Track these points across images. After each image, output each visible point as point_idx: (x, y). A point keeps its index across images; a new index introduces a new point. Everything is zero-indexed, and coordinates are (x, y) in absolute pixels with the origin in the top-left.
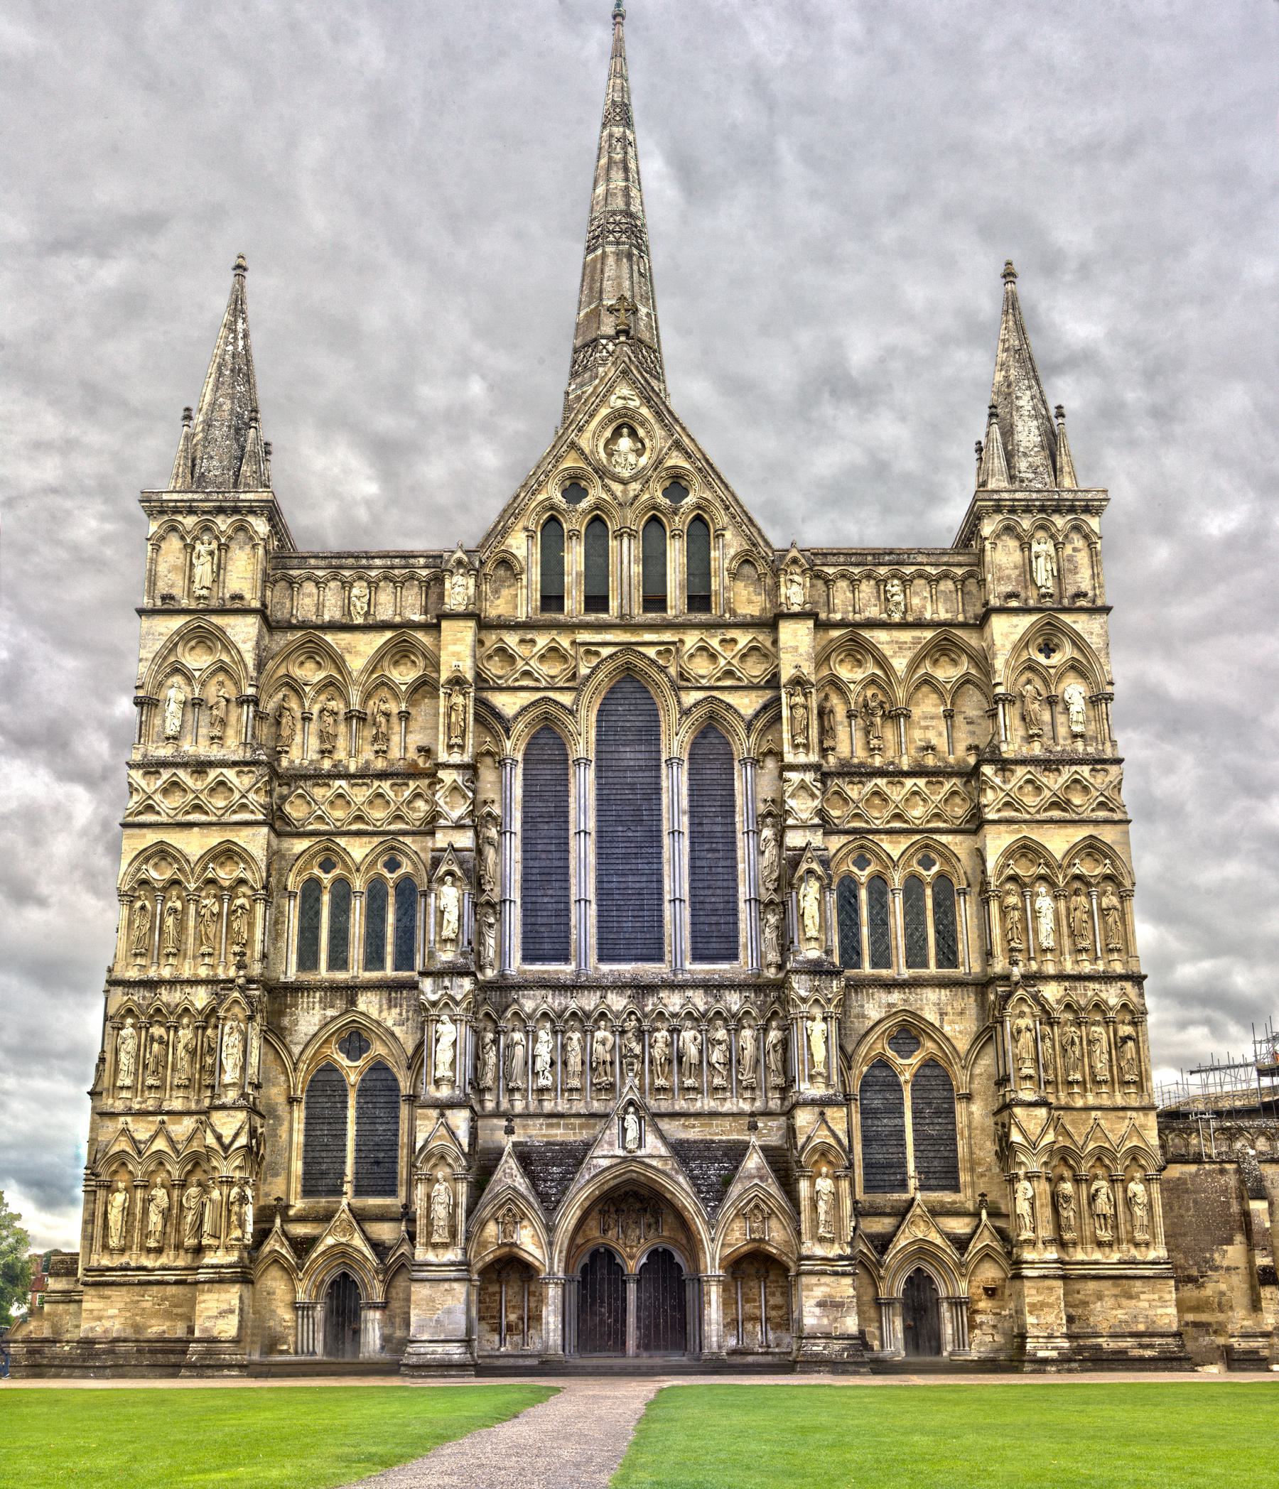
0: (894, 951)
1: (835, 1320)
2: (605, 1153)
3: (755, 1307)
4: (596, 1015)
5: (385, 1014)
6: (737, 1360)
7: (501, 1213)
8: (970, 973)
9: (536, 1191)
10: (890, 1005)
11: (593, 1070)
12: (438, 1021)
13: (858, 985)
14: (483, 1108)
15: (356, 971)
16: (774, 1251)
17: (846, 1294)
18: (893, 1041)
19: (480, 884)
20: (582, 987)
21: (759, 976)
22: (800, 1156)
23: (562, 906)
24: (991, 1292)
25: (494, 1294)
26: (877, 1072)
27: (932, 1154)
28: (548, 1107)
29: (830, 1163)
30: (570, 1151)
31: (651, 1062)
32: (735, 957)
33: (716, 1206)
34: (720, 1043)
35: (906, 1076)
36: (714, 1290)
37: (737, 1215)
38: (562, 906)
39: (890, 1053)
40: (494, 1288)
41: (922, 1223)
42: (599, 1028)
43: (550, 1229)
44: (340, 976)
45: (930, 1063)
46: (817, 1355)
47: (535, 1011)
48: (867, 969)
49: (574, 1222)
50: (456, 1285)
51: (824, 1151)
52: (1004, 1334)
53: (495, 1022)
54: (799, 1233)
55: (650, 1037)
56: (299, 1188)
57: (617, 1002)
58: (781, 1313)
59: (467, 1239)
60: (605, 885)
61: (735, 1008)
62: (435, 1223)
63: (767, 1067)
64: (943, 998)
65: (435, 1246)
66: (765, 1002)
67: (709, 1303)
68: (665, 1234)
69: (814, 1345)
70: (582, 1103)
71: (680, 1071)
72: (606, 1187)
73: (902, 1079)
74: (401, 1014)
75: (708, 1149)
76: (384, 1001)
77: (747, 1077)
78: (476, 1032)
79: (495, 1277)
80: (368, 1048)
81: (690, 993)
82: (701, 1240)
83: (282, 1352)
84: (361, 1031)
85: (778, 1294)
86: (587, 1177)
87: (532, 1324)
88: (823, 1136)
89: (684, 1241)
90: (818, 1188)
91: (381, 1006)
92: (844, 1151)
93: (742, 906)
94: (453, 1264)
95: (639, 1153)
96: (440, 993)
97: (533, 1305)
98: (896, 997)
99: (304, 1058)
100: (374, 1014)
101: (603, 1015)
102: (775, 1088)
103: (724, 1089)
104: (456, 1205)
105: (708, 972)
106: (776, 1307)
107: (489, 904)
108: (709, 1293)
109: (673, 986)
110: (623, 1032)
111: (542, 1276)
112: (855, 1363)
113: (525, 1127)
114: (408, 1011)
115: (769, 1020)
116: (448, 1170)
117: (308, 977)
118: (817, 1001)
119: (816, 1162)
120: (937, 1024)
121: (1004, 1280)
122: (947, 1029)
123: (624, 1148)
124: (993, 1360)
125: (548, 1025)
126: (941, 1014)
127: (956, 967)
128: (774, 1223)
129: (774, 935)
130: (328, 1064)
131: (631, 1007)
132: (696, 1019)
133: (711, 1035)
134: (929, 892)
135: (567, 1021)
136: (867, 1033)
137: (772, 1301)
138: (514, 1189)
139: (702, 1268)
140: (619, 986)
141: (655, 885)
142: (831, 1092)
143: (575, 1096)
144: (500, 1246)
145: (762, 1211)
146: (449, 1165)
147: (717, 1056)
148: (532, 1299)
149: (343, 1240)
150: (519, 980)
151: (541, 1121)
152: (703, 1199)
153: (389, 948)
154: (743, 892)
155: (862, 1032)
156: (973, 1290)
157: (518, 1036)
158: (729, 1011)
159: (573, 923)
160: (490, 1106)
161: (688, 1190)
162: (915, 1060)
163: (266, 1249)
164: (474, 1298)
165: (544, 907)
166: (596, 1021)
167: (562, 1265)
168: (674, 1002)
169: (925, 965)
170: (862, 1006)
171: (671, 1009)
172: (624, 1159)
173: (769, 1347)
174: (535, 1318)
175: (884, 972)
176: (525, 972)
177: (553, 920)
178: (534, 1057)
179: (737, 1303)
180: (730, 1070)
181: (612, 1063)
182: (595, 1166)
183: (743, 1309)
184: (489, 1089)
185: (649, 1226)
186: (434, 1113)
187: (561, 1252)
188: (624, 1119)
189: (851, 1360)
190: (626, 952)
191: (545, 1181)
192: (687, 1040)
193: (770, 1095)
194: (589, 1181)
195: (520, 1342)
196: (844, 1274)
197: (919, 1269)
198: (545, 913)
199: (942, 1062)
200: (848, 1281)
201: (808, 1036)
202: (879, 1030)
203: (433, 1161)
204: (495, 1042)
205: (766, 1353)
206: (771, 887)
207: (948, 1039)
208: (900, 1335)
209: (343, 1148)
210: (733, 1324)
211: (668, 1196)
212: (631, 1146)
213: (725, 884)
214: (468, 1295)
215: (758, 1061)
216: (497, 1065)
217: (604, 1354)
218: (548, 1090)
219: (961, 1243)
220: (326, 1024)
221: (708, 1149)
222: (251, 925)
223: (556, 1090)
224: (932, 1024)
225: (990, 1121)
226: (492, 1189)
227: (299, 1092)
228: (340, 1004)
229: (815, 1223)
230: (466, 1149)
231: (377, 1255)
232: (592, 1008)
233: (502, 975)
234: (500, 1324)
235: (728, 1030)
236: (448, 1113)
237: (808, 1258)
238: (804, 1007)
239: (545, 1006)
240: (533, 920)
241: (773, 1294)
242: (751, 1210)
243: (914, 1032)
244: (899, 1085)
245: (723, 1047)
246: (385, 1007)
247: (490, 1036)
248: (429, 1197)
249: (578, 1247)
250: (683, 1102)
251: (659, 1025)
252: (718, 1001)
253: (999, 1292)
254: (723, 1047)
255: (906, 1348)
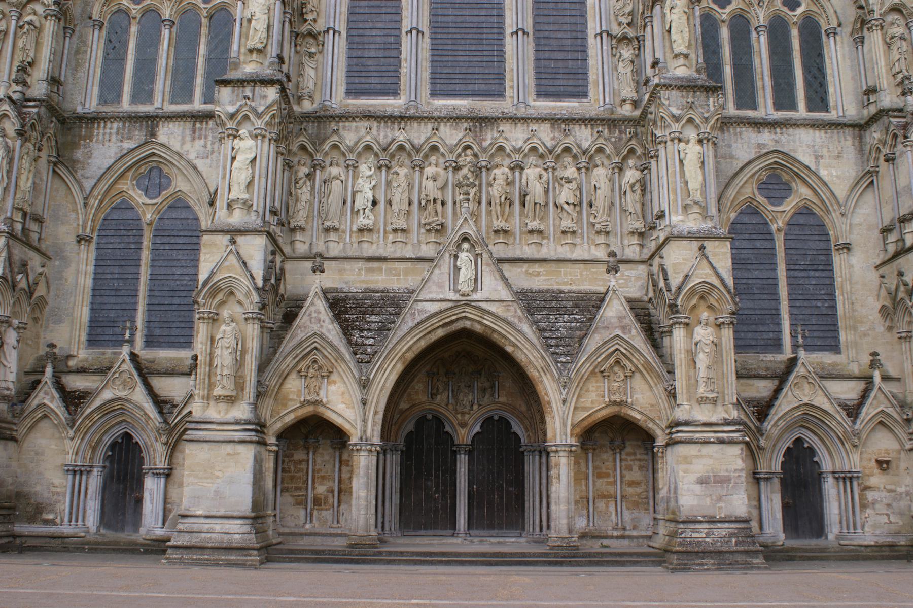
0: (760, 93)
1: (720, 499)
2: (433, 296)
3: (608, 483)
4: (426, 148)
5: (187, 146)
6: (595, 546)
7: (303, 365)
8: (844, 116)
9: (349, 341)
10: (759, 145)
11: (422, 208)
12: (235, 137)
13: (726, 123)
14: (293, 250)
15: (160, 102)
16: (638, 416)
17: (733, 467)
18: (764, 187)
19: (302, 14)
20: (411, 118)
21: (612, 113)
22: (676, 299)
23: (392, 39)
24: (883, 465)
25: (301, 462)
26: (746, 219)
27: (808, 311)
28: (369, 250)
29: (711, 307)
30: (393, 298)
31: (490, 203)
32: (585, 95)
33: (567, 362)
34: (569, 181)
35: (778, 224)
36: (563, 461)
37: (593, 373)
38: (392, 39)
39: (760, 199)
40: (299, 455)
41: (806, 386)
42: (430, 164)
43: (364, 385)
44: (143, 108)
45: (805, 211)
46: (699, 543)
47: (356, 144)
48: (732, 110)
49: (394, 377)
50: (241, 448)
51: (703, 294)
52: (901, 514)
53: (311, 156)
54: (672, 395)
55: (488, 175)
56: (84, 337)
57: (451, 135)
58: (639, 490)
59: (259, 395)
60: (440, 19)
61: (585, 145)
62: (219, 371)
63: (624, 210)
64: (818, 140)
65: (218, 399)
66: (620, 139)
67: (559, 477)
68: (503, 399)
69: (694, 531)
70: (409, 247)
71: (522, 214)
72: (434, 337)
73: (774, 227)
74: (205, 146)
75: (556, 299)
76: (188, 133)
77: (601, 219)
78: (288, 166)
79: (302, 443)
80: (169, 184)
81: (534, 126)
82: (549, 403)
83: (46, 522)
84: (163, 167)
85: (635, 468)
86: (411, 324)
87: (343, 497)
88: (703, 274)
89: (524, 408)
90: (697, 338)
91: (183, 138)
92: (729, 292)
93: (593, 45)
94: (237, 423)
95: (475, 297)
96: (239, 103)
97: (345, 476)
98: (766, 138)
99: (96, 193)
100: (176, 145)
101: (434, 149)
102: (632, 233)
103: (574, 233)
104: (244, 352)
105: (554, 108)
106: (632, 484)
107: (312, 35)
108: (558, 465)
109: (514, 120)
110: (457, 169)
111: (354, 440)
112: (746, 552)
113: (340, 271)
114: (213, 143)
115: (625, 158)
116: (238, 309)
117: (109, 109)
118: (690, 121)
119: (694, 307)
120: (813, 168)
121: (899, 452)
122: (823, 173)
123: (457, 291)
124: (892, 546)
125: (372, 158)
126: (816, 158)
127: (827, 111)
128: (638, 381)
129: (629, 70)
130: (124, 201)
131: (469, 140)
132: (542, 156)
133: (560, 173)
134: (795, 32)
135: (392, 156)
136: (736, 175)
137: (628, 477)
138: (321, 336)
139: (549, 435)
140: (455, 119)
141: (495, 19)
142: (709, 224)
143: (400, 237)
144: (302, 405)
145: (624, 368)
146: (239, 302)
147: (565, 195)
148: (344, 468)
149: (123, 394)
150: (339, 111)
151: (360, 264)
152: (553, 354)
153: (199, 80)
154: (593, 27)
155: (730, 174)
156: (865, 463)
157: (335, 171)
158: (579, 147)
159: (403, 56)
160: (301, 248)
161: (535, 340)
162: (789, 206)
163: (34, 402)
164: (269, 464)
165: (371, 39)
166: (426, 156)
167: (378, 428)
168: (516, 136)
169: (793, 107)
170: (730, 146)
171: (514, 143)
172: (457, 304)
173: (624, 529)
174: (344, 491)
175: (750, 113)
176: (348, 105)
177: (381, 54)
178: (354, 194)
179: (587, 478)
180: (580, 213)
181: (443, 204)
182: (420, 311)
183: (593, 486)
184: (302, 229)
185: (484, 390)
186: (225, 239)
187: (376, 413)
188: (456, 257)
189: (741, 548)
190: (463, 87)
191: (361, 331)
192: (531, 177)
193: (626, 242)
194: (412, 329)
195: (330, 518)
196: (732, 442)
197: (799, 441)
198: (372, 46)
199: (817, 210)
200: (736, 450)
201: (681, 162)
202: (748, 172)
203: (220, 297)
204: (309, 176)
205: (622, 537)
206: (625, 20)
207: (825, 184)
208: (779, 515)
209: (134, 294)
210: (584, 502)
211: (509, 349)
212: (465, 287)
213: (572, 20)
214: (258, 462)
215: (612, 204)
216: (311, 203)
217: (430, 532)
218: (370, 230)
219: (853, 411)
220: (122, 157)
221: (556, 299)
222: (38, 44)
223: (379, 232)
224: (807, 167)
225: (873, 276)
226: (297, 335)
227: (88, 230)
228: (139, 135)
229: (693, 384)
230: (260, 283)
231: (161, 412)
232: (422, 141)
233: (324, 108)
234: (306, 496)
235: (579, 169)
236: (240, 239)
237: (687, 423)
238: (676, 127)
239: (368, 138)
240: (359, 53)
241: (629, 468)
242: (611, 367)
243: (785, 177)
244: (771, 234)
245: (573, 185)
246: (188, 138)
247: (303, 171)
248: (212, 340)
249: (402, 412)
250: (526, 247)
251: (498, 160)
252: (566, 135)
253: (893, 465)
254: (573, 185)
255: (784, 531)
